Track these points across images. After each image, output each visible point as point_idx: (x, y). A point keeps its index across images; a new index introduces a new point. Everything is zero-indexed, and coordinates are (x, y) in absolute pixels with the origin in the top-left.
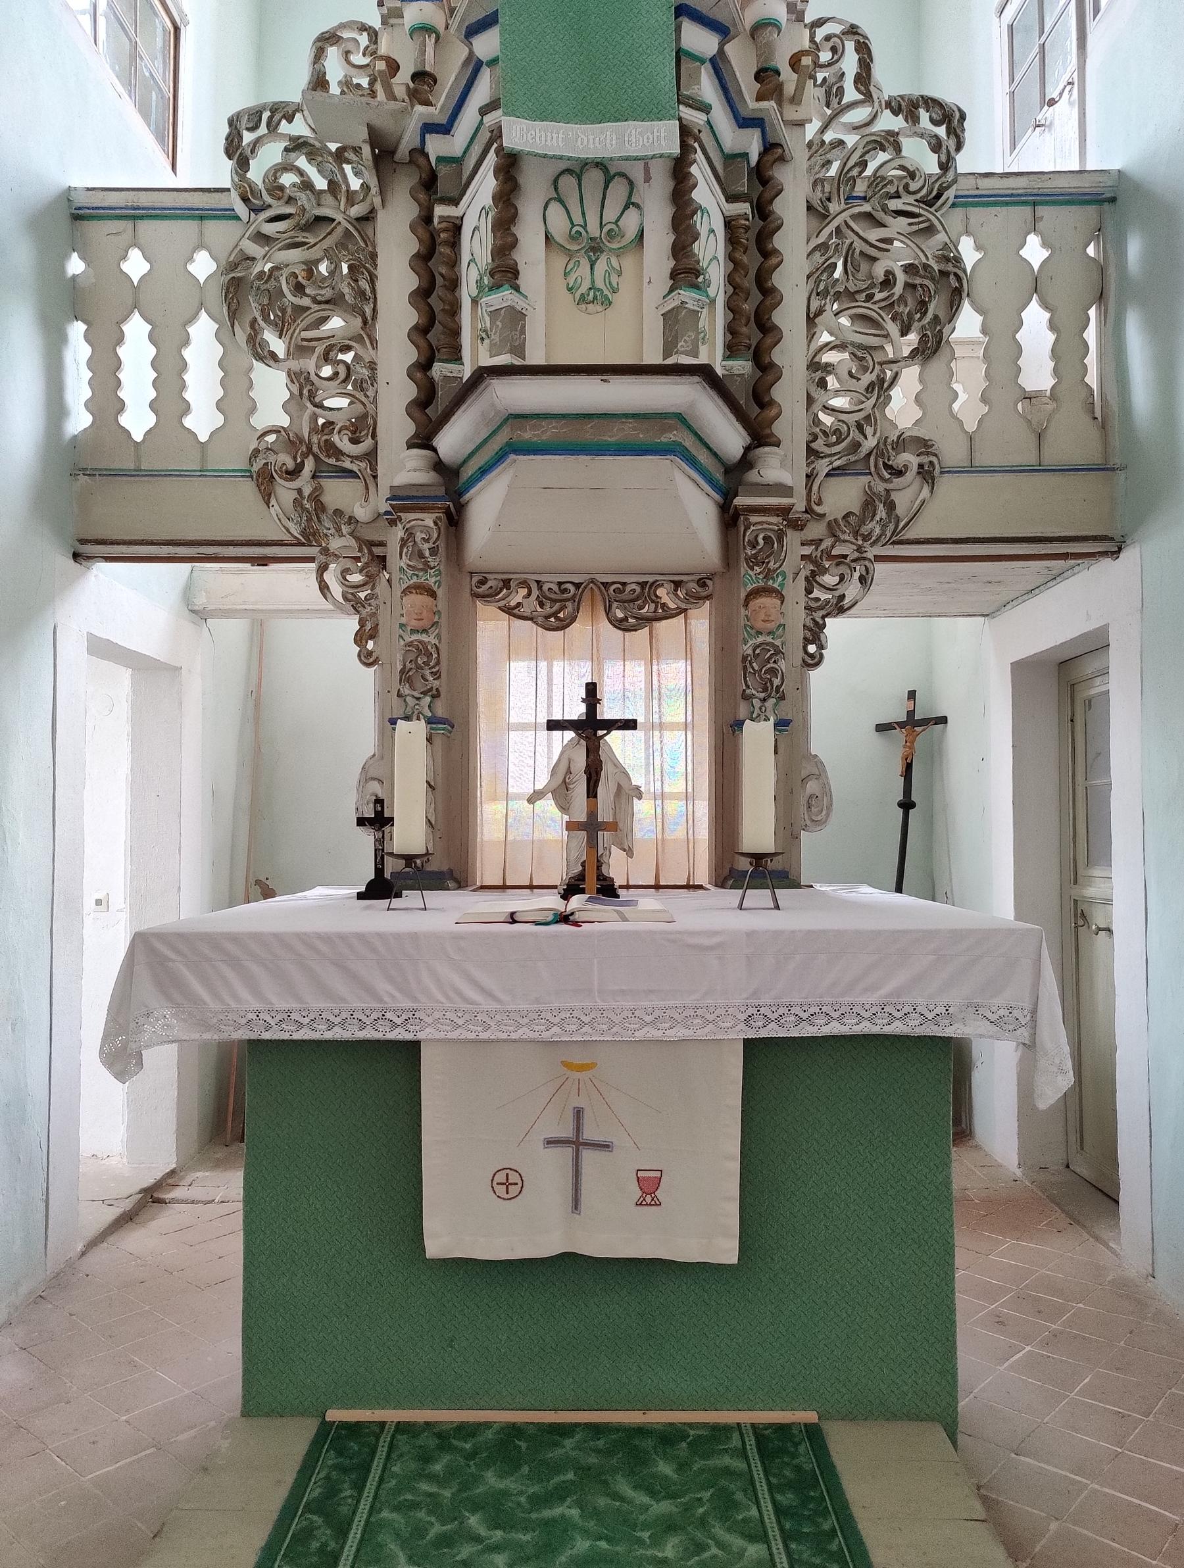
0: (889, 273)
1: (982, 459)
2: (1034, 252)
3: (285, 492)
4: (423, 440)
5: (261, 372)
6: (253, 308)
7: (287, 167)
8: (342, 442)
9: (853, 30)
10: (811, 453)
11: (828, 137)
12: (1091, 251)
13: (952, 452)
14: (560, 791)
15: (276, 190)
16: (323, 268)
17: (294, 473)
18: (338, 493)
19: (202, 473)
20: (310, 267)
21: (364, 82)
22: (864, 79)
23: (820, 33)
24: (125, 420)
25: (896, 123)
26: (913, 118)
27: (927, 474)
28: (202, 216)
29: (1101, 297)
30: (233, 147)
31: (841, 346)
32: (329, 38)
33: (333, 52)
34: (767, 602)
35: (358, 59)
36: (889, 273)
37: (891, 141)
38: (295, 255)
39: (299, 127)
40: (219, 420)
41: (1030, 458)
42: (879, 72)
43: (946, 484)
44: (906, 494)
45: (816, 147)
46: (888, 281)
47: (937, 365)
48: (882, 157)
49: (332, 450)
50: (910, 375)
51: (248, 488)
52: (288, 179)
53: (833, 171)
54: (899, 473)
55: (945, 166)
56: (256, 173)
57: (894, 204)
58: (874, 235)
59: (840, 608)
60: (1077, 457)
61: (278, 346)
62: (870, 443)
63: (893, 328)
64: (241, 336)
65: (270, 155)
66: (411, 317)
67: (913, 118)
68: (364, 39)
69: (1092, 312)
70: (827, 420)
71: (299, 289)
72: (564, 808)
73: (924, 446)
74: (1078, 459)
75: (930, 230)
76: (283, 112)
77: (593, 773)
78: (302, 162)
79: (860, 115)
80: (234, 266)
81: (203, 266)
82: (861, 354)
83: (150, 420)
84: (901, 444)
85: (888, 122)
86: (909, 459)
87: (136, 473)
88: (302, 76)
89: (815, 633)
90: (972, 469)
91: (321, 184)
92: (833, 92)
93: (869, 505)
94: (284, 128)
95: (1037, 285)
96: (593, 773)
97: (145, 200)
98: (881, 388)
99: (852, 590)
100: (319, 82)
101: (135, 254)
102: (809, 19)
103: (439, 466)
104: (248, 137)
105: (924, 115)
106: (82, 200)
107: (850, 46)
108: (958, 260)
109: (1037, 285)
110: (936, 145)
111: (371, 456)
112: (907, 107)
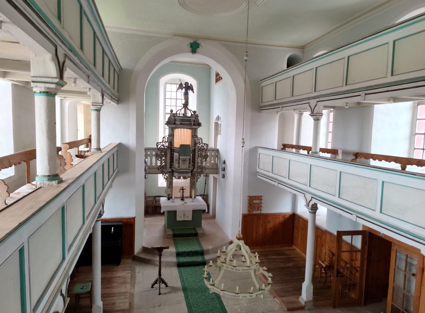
1: (209, 168)
2: (213, 154)
3: (160, 170)
4: (171, 168)
5: (158, 161)
7: (161, 147)
8: (164, 167)
9: (201, 138)
10: (197, 168)
11: (199, 146)
12: (217, 154)
13: (207, 167)
15: (160, 149)
16: (163, 153)
17: (161, 169)
18: (164, 170)
22: (202, 142)
23: (199, 139)
26: (205, 145)
27: (205, 169)
28: (154, 150)
29: (217, 157)
31: (200, 160)
33: (164, 138)
34: (194, 179)
36: (203, 156)
37: (203, 146)
42: (203, 142)
44: (203, 170)
45: (198, 146)
46: (203, 156)
47: (206, 161)
48: (203, 147)
49: (163, 167)
51: (157, 170)
52: (161, 148)
54: (203, 169)
55: (207, 148)
57: (203, 151)
58: (202, 153)
59: (199, 178)
61: (160, 159)
62: (201, 167)
65: (159, 146)
66: (170, 159)
67: (205, 145)
69: (217, 158)
70: (199, 165)
75: (206, 153)
76: (160, 143)
80: (157, 154)
81: (154, 153)
82: (201, 161)
83: (150, 164)
84: (203, 167)
85: (203, 145)
86: (204, 168)
88: (162, 140)
89: (197, 180)
90: (208, 169)
92: (200, 143)
93: (201, 171)
98: (202, 163)
99: (200, 177)
100: (163, 141)
101: (149, 152)
102: (198, 137)
103: (172, 169)
107: (201, 139)
110: (206, 147)
111: (166, 167)
112: (205, 144)
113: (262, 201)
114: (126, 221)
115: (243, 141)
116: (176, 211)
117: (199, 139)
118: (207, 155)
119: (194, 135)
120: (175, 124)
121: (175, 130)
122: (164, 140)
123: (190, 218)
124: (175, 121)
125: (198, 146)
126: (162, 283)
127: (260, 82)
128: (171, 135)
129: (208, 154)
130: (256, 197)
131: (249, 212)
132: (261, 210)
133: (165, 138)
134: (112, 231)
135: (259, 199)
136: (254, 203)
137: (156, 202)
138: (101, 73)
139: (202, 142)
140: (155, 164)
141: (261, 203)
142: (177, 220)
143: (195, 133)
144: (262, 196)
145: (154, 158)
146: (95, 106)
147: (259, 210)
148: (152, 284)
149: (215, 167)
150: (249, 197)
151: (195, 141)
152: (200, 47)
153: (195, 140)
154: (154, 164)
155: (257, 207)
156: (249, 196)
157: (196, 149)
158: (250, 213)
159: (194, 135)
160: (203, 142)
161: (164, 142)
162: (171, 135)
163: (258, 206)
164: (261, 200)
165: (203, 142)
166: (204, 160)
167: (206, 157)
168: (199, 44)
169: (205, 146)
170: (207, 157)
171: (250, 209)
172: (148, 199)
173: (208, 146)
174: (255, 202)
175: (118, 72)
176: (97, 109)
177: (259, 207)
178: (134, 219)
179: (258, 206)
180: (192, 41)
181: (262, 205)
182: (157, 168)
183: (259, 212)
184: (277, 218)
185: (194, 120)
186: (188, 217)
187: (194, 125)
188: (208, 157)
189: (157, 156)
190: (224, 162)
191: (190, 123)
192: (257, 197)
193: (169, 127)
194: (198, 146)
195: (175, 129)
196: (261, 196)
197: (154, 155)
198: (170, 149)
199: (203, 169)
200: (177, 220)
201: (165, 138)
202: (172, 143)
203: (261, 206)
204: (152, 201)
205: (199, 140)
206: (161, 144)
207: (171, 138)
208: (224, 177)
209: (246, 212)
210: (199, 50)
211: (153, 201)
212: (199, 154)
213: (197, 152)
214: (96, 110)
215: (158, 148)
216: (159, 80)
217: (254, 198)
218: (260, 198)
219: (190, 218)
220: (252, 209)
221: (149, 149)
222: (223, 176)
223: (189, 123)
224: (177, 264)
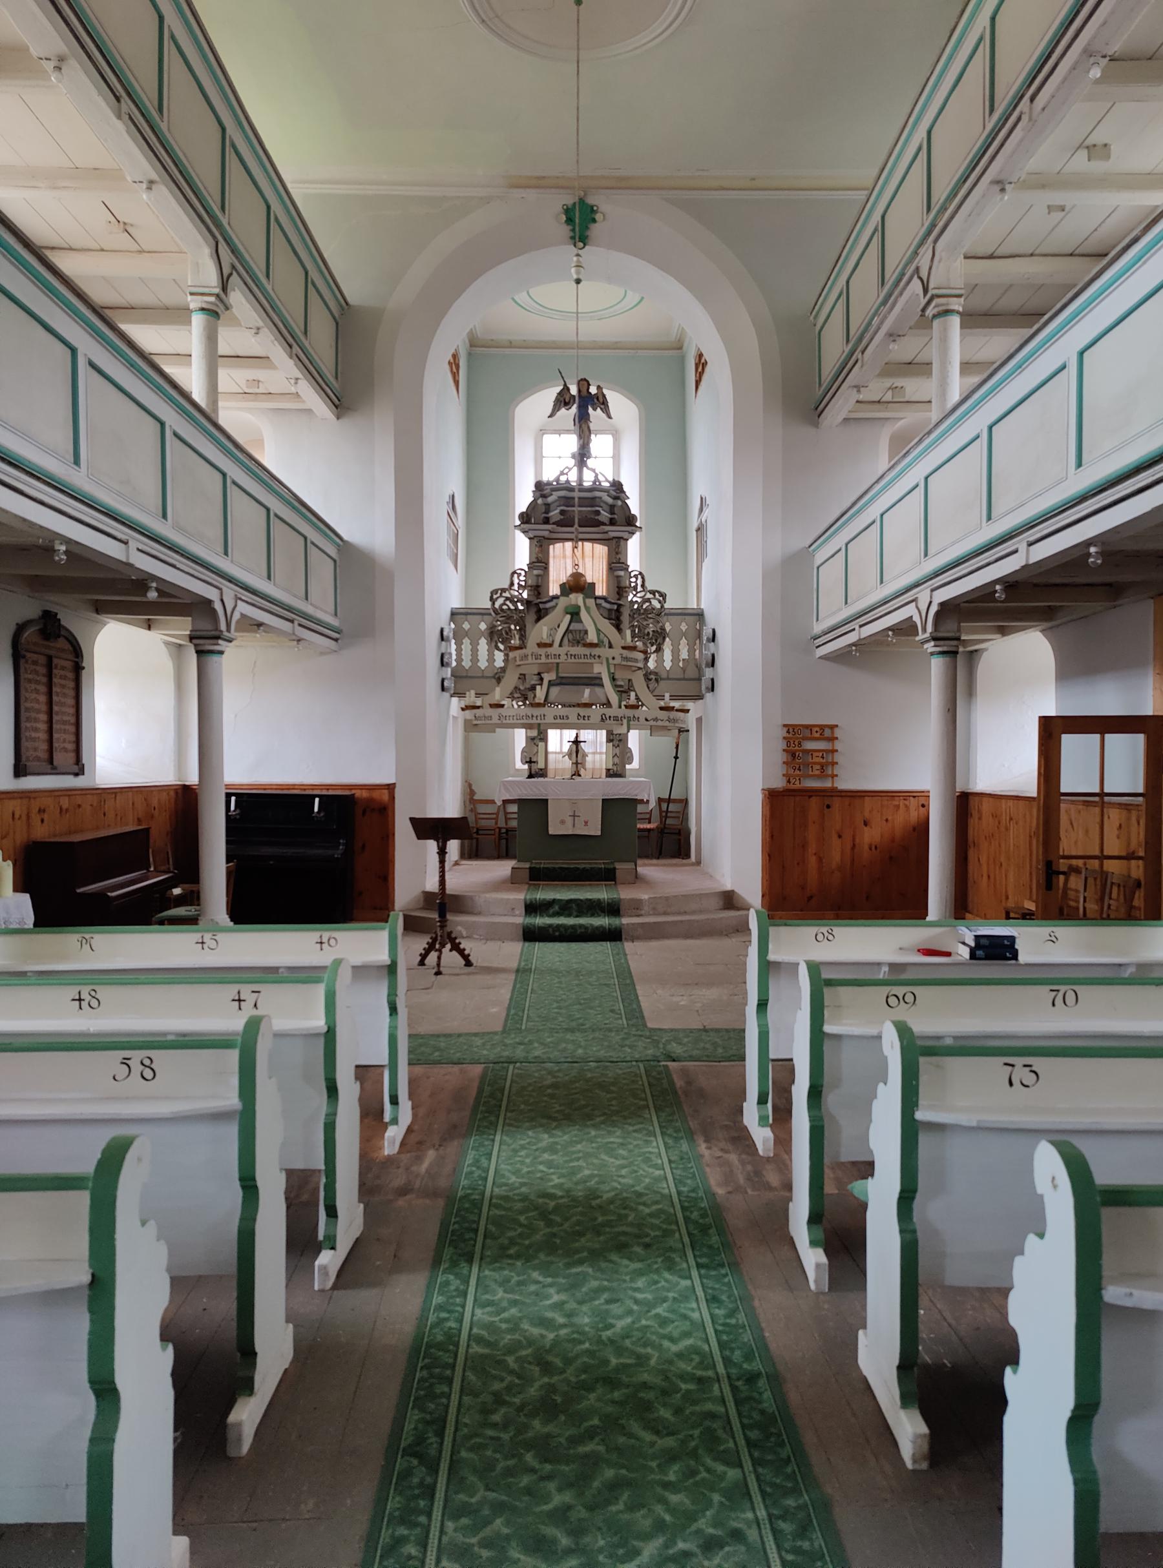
0: (648, 633)
5: (496, 652)
6: (496, 638)
7: (504, 604)
9: (640, 573)
11: (635, 599)
13: (664, 675)
14: (569, 754)
15: (502, 610)
16: (513, 627)
19: (483, 677)
20: (510, 628)
21: (523, 583)
24: (463, 664)
25: (651, 596)
27: (657, 680)
30: (491, 599)
32: (514, 572)
33: (516, 575)
35: (522, 578)
36: (648, 633)
37: (649, 600)
38: (506, 625)
39: (507, 594)
40: (487, 664)
41: (682, 676)
42: (647, 584)
43: (662, 683)
47: (660, 653)
48: (647, 604)
50: (653, 657)
52: (505, 607)
53: (636, 606)
54: (650, 680)
56: (497, 605)
58: (645, 623)
60: (692, 677)
61: (502, 647)
63: (649, 645)
64: (493, 644)
68: (523, 573)
71: (507, 634)
72: (570, 759)
73: (656, 674)
74: (692, 677)
75: (658, 622)
76: (503, 590)
77: (577, 752)
78: (508, 603)
79: (643, 594)
81: (483, 626)
83: (470, 664)
84: (650, 673)
85: (649, 596)
86: (652, 677)
87: (466, 677)
90: (668, 679)
91: (512, 607)
92: (635, 588)
94: (504, 594)
95: (684, 634)
96: (577, 752)
97: (469, 611)
98: (646, 660)
104: (495, 597)
105: (657, 594)
106: (454, 611)
108: (664, 630)
109: (684, 634)
110: (660, 602)
112: (653, 592)
113: (838, 745)
114: (365, 794)
115: (578, 261)
116: (544, 802)
117: (632, 574)
118: (663, 629)
119: (617, 563)
120: (546, 521)
121: (551, 547)
122: (516, 581)
123: (595, 829)
124: (547, 512)
125: (629, 599)
126: (451, 950)
127: (812, 318)
128: (539, 563)
129: (668, 627)
130: (815, 729)
131: (789, 782)
132: (833, 776)
133: (519, 575)
134: (316, 809)
135: (822, 738)
136: (807, 752)
137: (507, 819)
138: (218, 198)
139: (643, 586)
140: (487, 664)
141: (834, 751)
142: (552, 831)
143: (617, 553)
144: (837, 726)
145: (483, 644)
146: (199, 297)
147: (827, 776)
148: (421, 955)
149: (691, 672)
150: (785, 730)
151: (619, 582)
152: (598, 217)
153: (618, 577)
154: (483, 664)
155: (815, 763)
156: (785, 726)
157: (622, 610)
158: (792, 786)
159: (617, 563)
160: (649, 586)
161: (516, 587)
162: (539, 563)
163: (821, 760)
164: (833, 739)
165: (649, 586)
166: (654, 648)
167: (659, 637)
168: (592, 207)
169: (655, 598)
170: (664, 639)
171: (791, 771)
172: (482, 809)
173: (664, 599)
174: (810, 745)
175: (337, 315)
176: (205, 306)
177: (826, 764)
178: (391, 788)
179: (821, 760)
180: (569, 200)
181: (837, 758)
182: (494, 677)
183: (828, 784)
184: (898, 807)
185: (612, 507)
186: (586, 823)
187: (612, 522)
188: (667, 639)
189: (493, 635)
190: (713, 639)
191: (594, 509)
192: (818, 729)
193: (530, 538)
194: (629, 599)
195: (553, 544)
196: (833, 727)
197: (482, 634)
198: (533, 610)
199: (650, 680)
200: (552, 831)
201: (519, 575)
202: (541, 590)
203: (834, 764)
204: (494, 816)
205: (633, 580)
206: (507, 594)
207: (536, 572)
208: (713, 690)
209: (779, 783)
210: (596, 230)
211: (497, 814)
212: (633, 626)
213: (625, 618)
214: (203, 309)
215: (495, 610)
216: (514, 412)
217: (807, 733)
218: (827, 733)
219: (595, 829)
220: (797, 772)
221: (467, 614)
222: (710, 686)
223: (589, 509)
224: (521, 933)
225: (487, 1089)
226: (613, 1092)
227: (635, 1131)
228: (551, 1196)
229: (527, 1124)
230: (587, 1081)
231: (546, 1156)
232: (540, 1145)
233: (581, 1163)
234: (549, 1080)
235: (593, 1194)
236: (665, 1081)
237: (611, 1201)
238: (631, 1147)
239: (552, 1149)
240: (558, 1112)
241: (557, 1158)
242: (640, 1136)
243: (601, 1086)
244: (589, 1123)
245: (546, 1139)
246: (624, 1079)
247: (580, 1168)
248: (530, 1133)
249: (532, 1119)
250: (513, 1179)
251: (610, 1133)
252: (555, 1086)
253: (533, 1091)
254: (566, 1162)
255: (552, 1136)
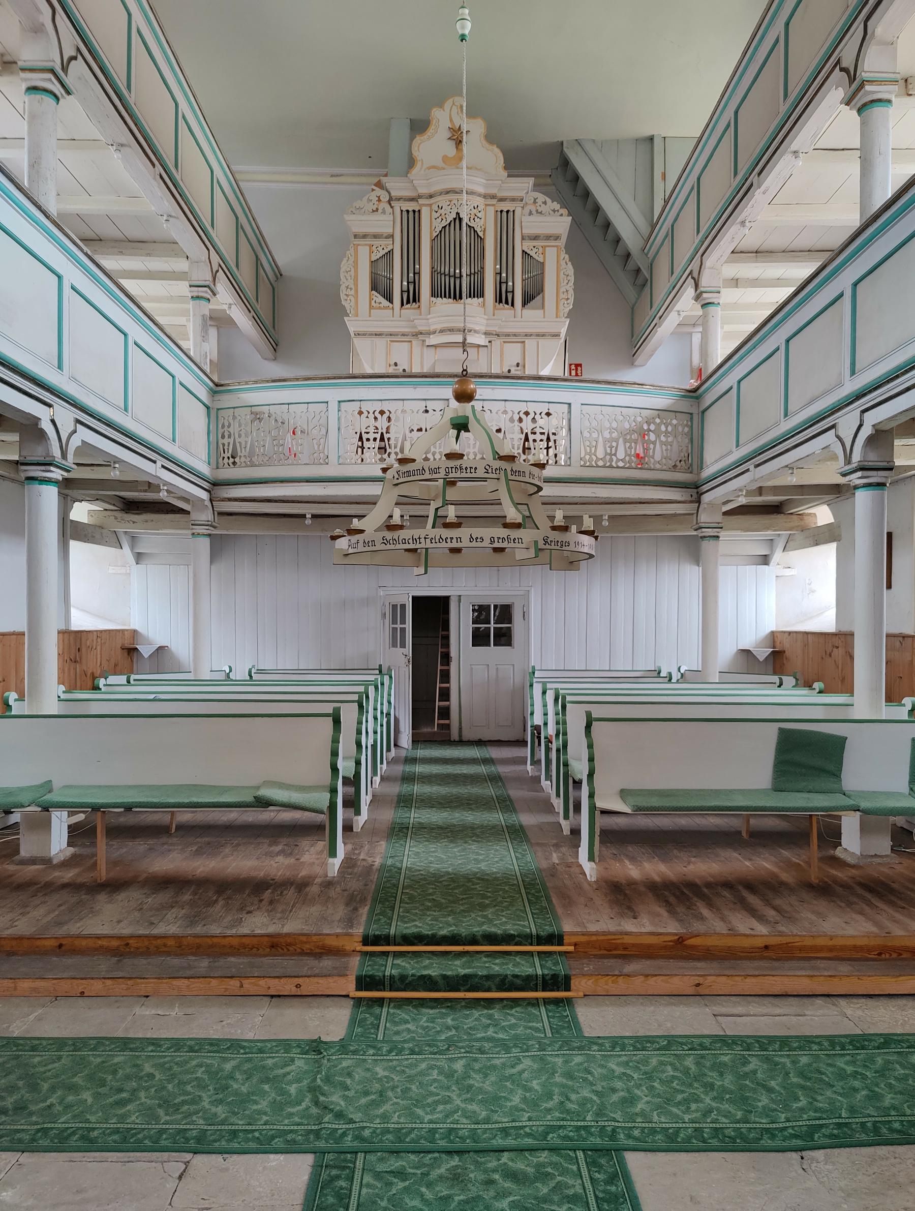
225: (544, 904)
226: (429, 900)
227: (420, 871)
228: (474, 841)
229: (498, 875)
230: (452, 912)
231: (481, 857)
232: (486, 863)
233: (459, 854)
234: (489, 912)
235: (451, 842)
236: (377, 911)
237: (444, 838)
238: (426, 862)
239: (477, 861)
240: (478, 884)
241: (472, 856)
242: (418, 868)
243: (438, 906)
244: (453, 876)
245: (483, 866)
246: (416, 914)
247: (459, 852)
248: (495, 870)
249: (496, 879)
250: (498, 848)
251: (438, 870)
252: (483, 907)
253: (501, 902)
254: (472, 898)
255: (479, 868)
